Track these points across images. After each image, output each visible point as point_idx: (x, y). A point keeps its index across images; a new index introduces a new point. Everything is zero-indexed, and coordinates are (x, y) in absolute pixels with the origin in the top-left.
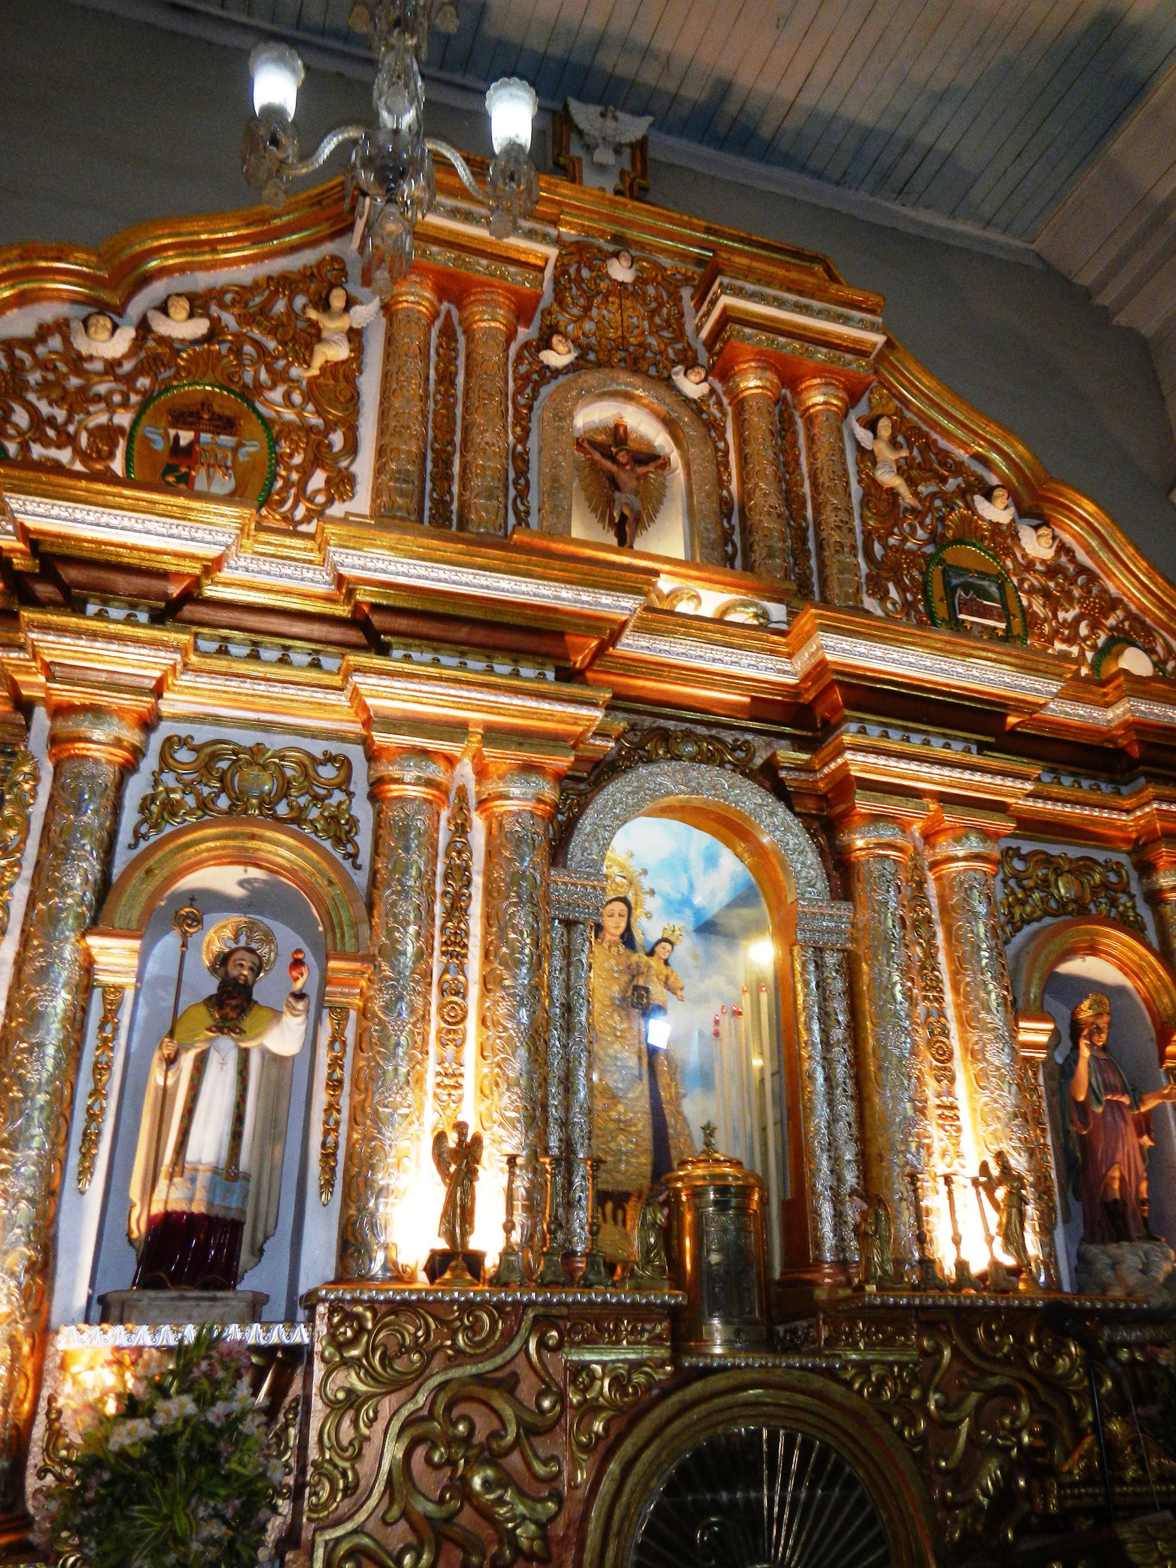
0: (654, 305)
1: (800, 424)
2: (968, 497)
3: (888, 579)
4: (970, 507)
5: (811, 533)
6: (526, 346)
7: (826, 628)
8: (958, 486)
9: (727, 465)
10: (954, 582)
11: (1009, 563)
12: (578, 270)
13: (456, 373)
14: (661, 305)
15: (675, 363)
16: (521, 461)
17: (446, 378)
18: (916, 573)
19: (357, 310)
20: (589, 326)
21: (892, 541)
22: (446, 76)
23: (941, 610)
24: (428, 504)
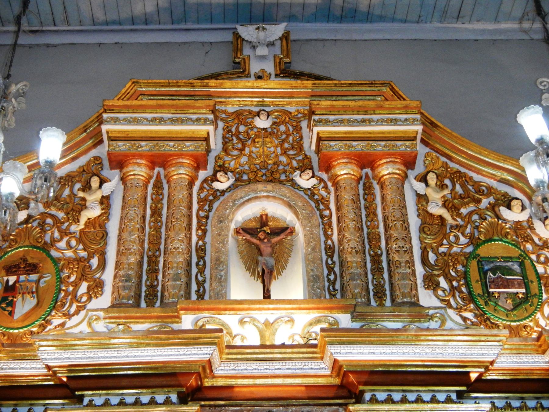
0: (284, 136)
1: (377, 188)
2: (496, 209)
3: (439, 276)
4: (498, 217)
5: (384, 258)
6: (205, 181)
7: (331, 344)
8: (490, 204)
9: (330, 225)
10: (486, 268)
11: (529, 246)
12: (237, 128)
13: (162, 208)
14: (288, 136)
15: (295, 169)
16: (201, 250)
17: (156, 213)
18: (460, 267)
19: (106, 185)
20: (244, 159)
21: (442, 249)
22: (175, 27)
23: (477, 289)
24: (144, 288)
